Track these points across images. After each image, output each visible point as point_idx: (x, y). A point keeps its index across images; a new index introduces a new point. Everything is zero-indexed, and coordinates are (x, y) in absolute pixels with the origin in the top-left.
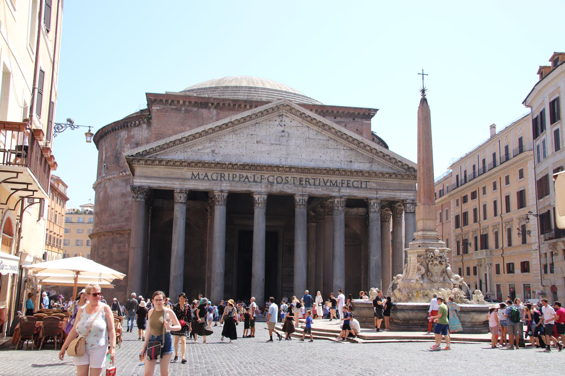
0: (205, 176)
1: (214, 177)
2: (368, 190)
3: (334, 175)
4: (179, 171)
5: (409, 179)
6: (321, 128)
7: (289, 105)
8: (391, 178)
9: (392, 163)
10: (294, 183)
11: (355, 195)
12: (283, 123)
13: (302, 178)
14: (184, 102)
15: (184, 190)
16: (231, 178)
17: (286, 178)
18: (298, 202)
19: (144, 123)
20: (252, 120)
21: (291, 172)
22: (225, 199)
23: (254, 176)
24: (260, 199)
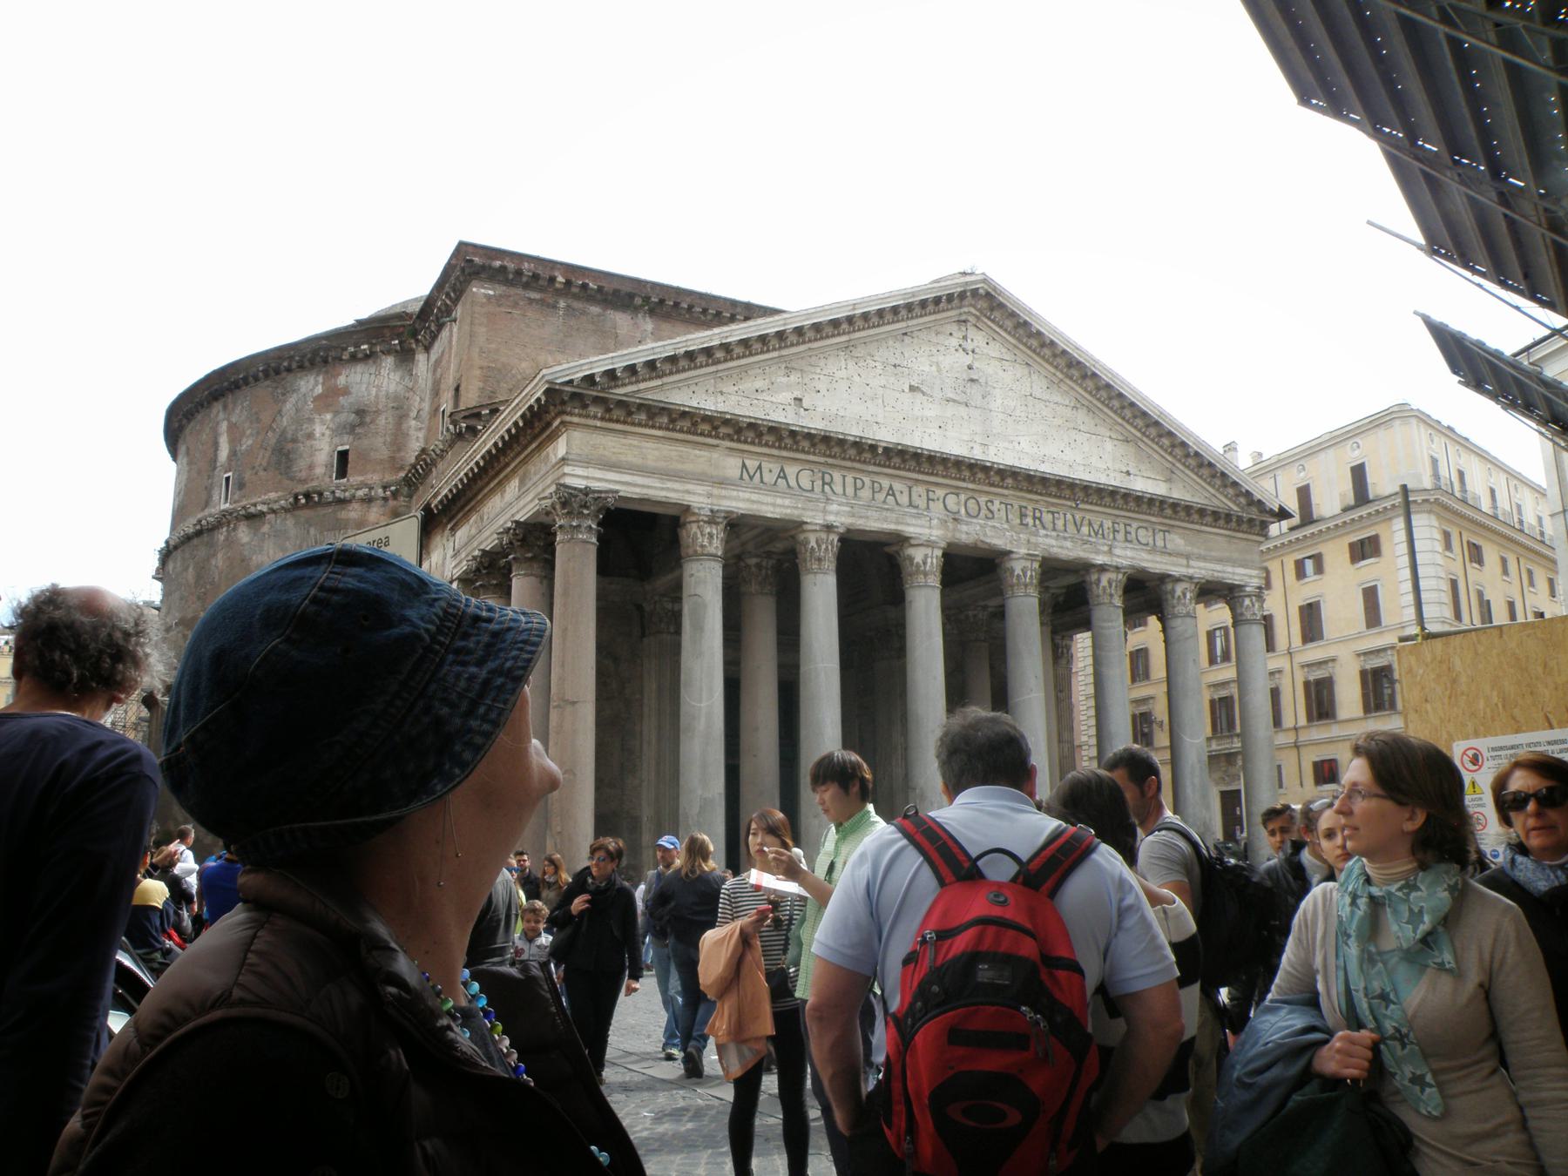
0: (779, 477)
1: (805, 482)
2: (1170, 554)
3: (1100, 505)
4: (702, 453)
5: (1250, 533)
6: (1061, 371)
7: (993, 293)
8: (1215, 527)
9: (1213, 487)
10: (1007, 521)
11: (1144, 564)
12: (969, 345)
13: (1026, 508)
14: (568, 283)
15: (723, 515)
16: (850, 491)
17: (989, 504)
18: (1018, 576)
19: (387, 352)
20: (898, 321)
21: (1002, 487)
23: (910, 488)
24: (929, 560)
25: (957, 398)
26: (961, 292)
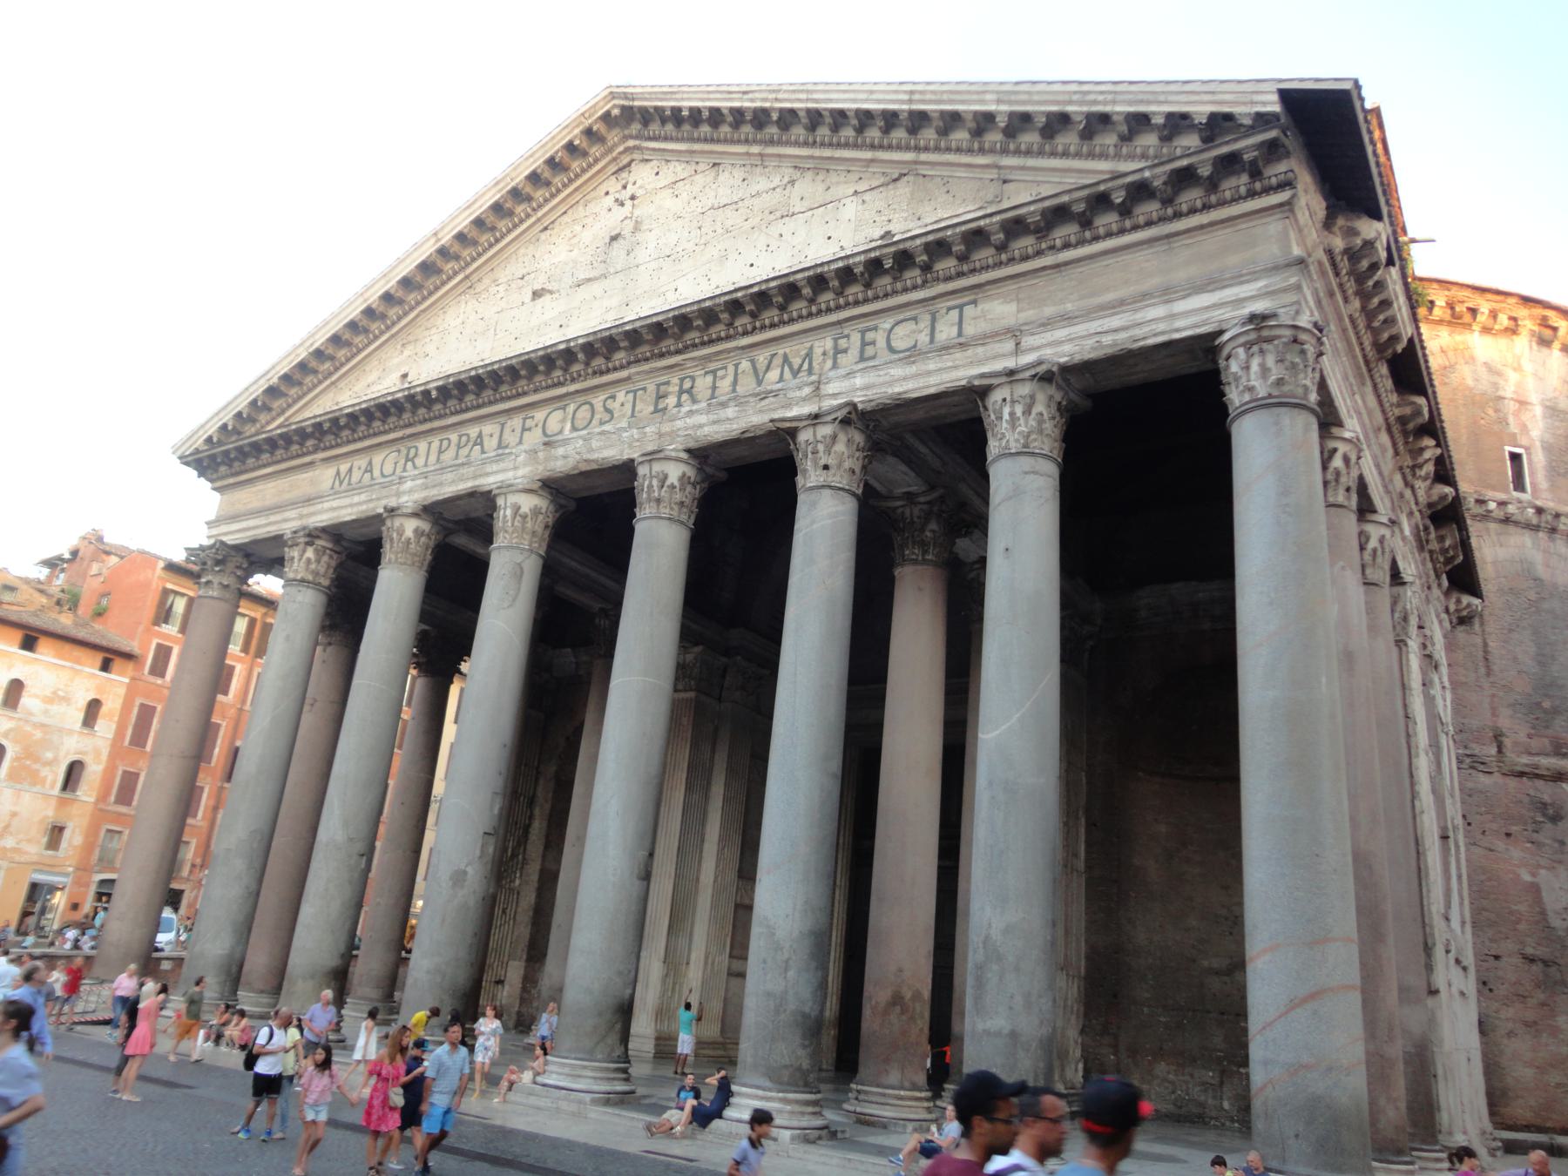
0: (366, 471)
3: (792, 321)
5: (1223, 203)
6: (755, 142)
7: (626, 103)
8: (1096, 238)
9: (1103, 156)
10: (633, 415)
11: (897, 390)
13: (668, 383)
15: (302, 533)
16: (433, 458)
17: (609, 401)
20: (522, 221)
21: (615, 369)
22: (408, 541)
25: (591, 276)
26: (589, 132)
